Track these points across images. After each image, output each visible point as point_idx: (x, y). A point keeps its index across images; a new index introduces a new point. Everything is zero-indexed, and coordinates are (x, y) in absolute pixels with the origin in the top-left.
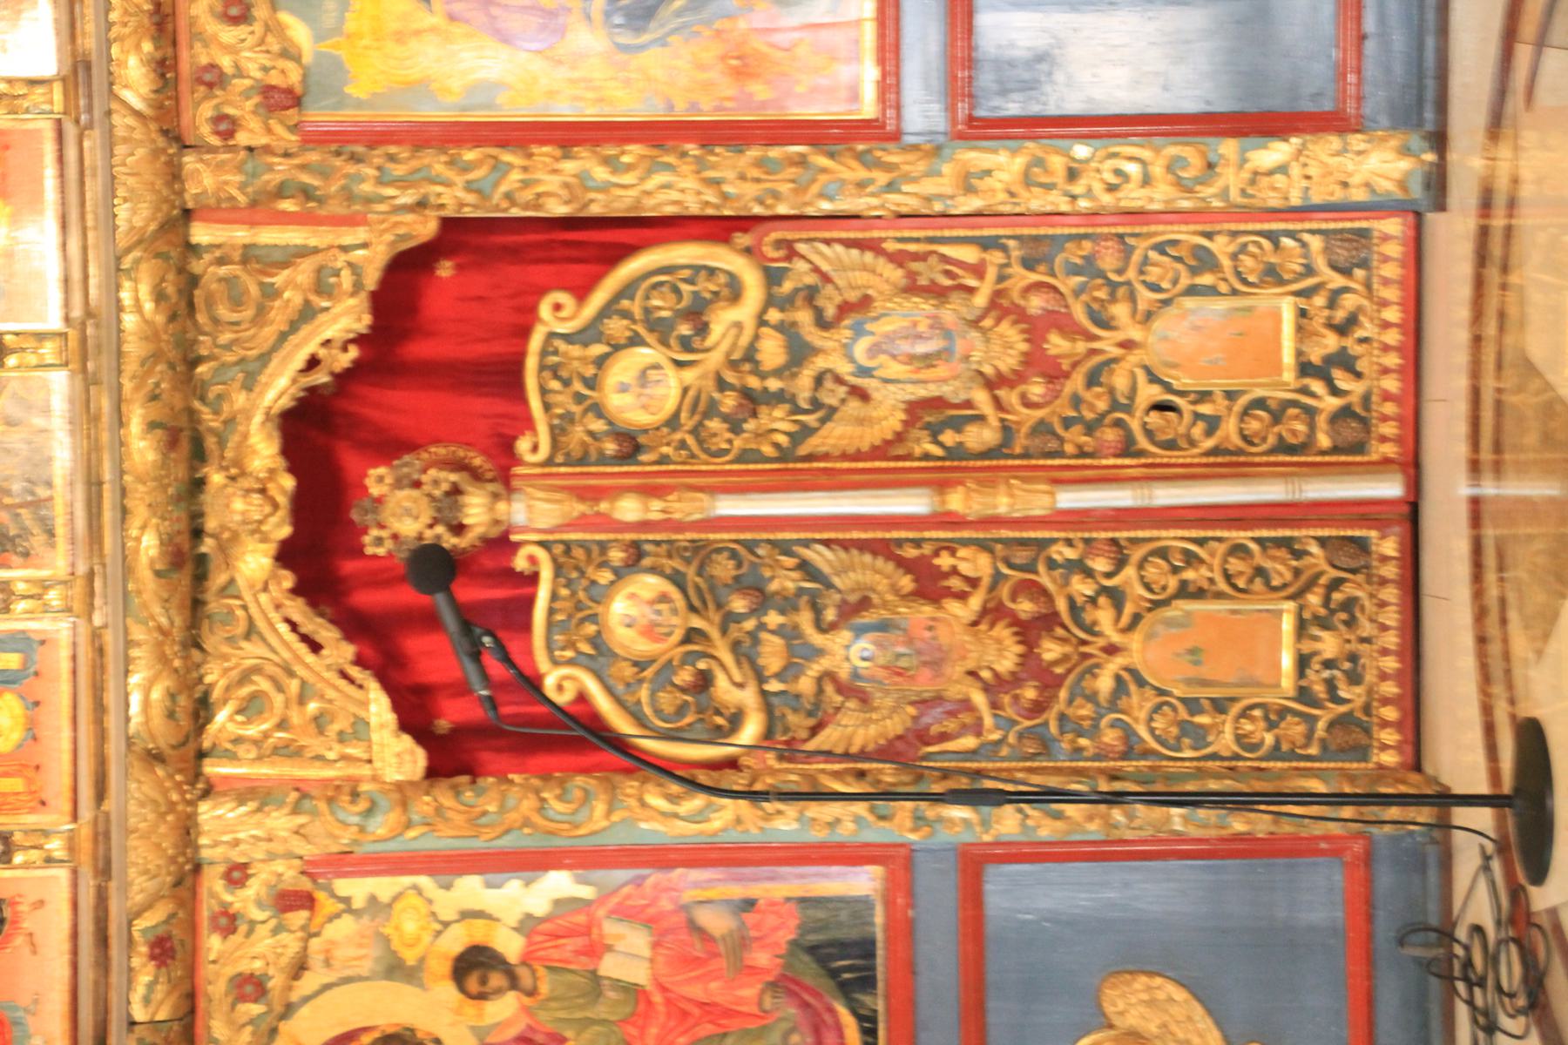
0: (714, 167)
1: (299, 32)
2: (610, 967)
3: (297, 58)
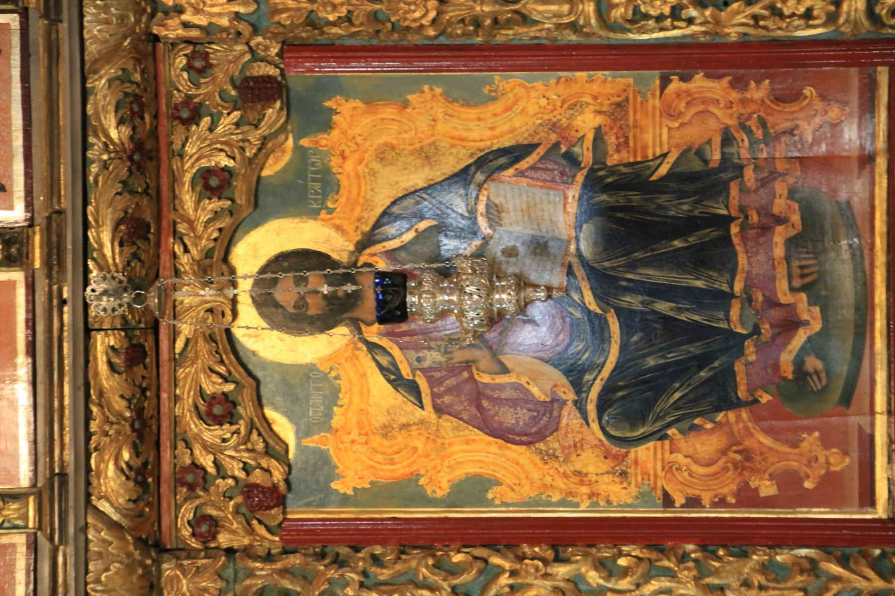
0: (716, 573)
3: (282, 456)
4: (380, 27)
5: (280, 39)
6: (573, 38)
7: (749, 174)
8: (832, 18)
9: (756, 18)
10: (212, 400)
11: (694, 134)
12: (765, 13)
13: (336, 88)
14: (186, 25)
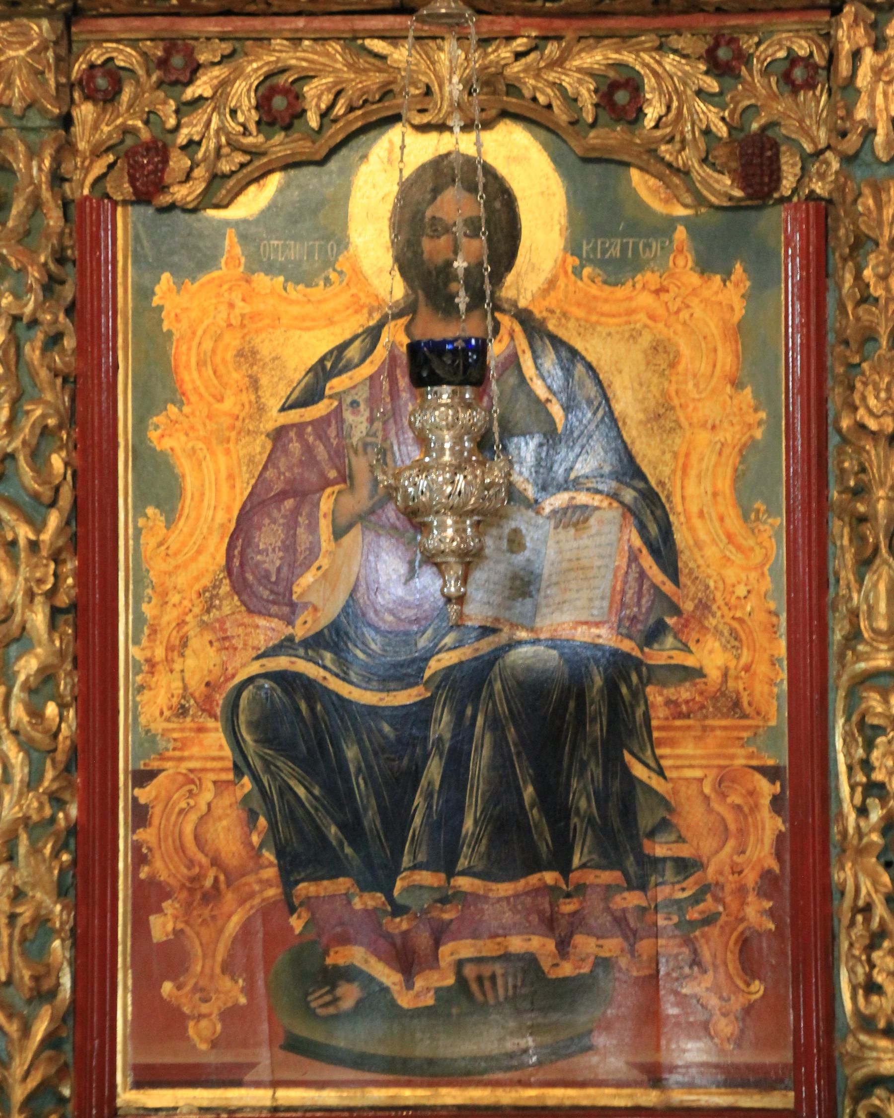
0: (35, 850)
1: (253, 202)
4: (854, 346)
5: (836, 196)
6: (837, 636)
7: (632, 899)
8: (867, 1023)
9: (867, 909)
10: (294, 95)
11: (693, 816)
12: (875, 924)
13: (763, 280)
14: (856, 55)
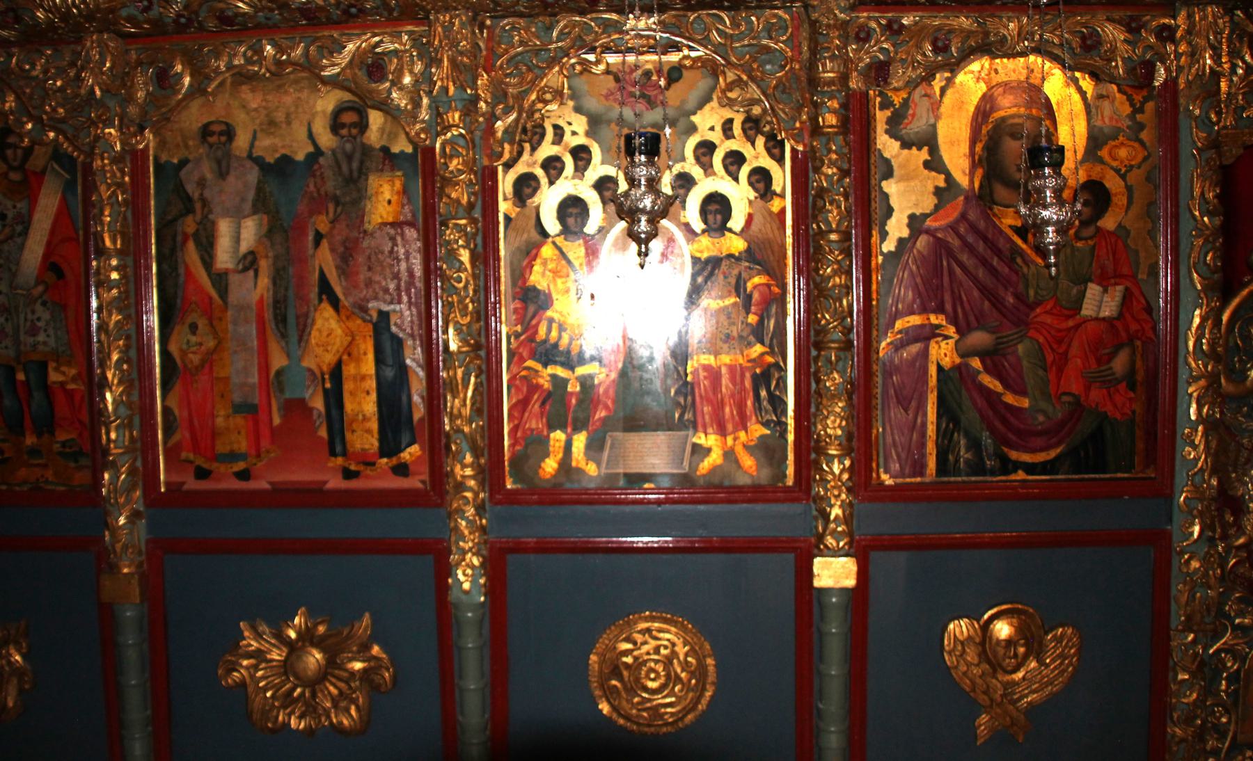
2: (1093, 290)
